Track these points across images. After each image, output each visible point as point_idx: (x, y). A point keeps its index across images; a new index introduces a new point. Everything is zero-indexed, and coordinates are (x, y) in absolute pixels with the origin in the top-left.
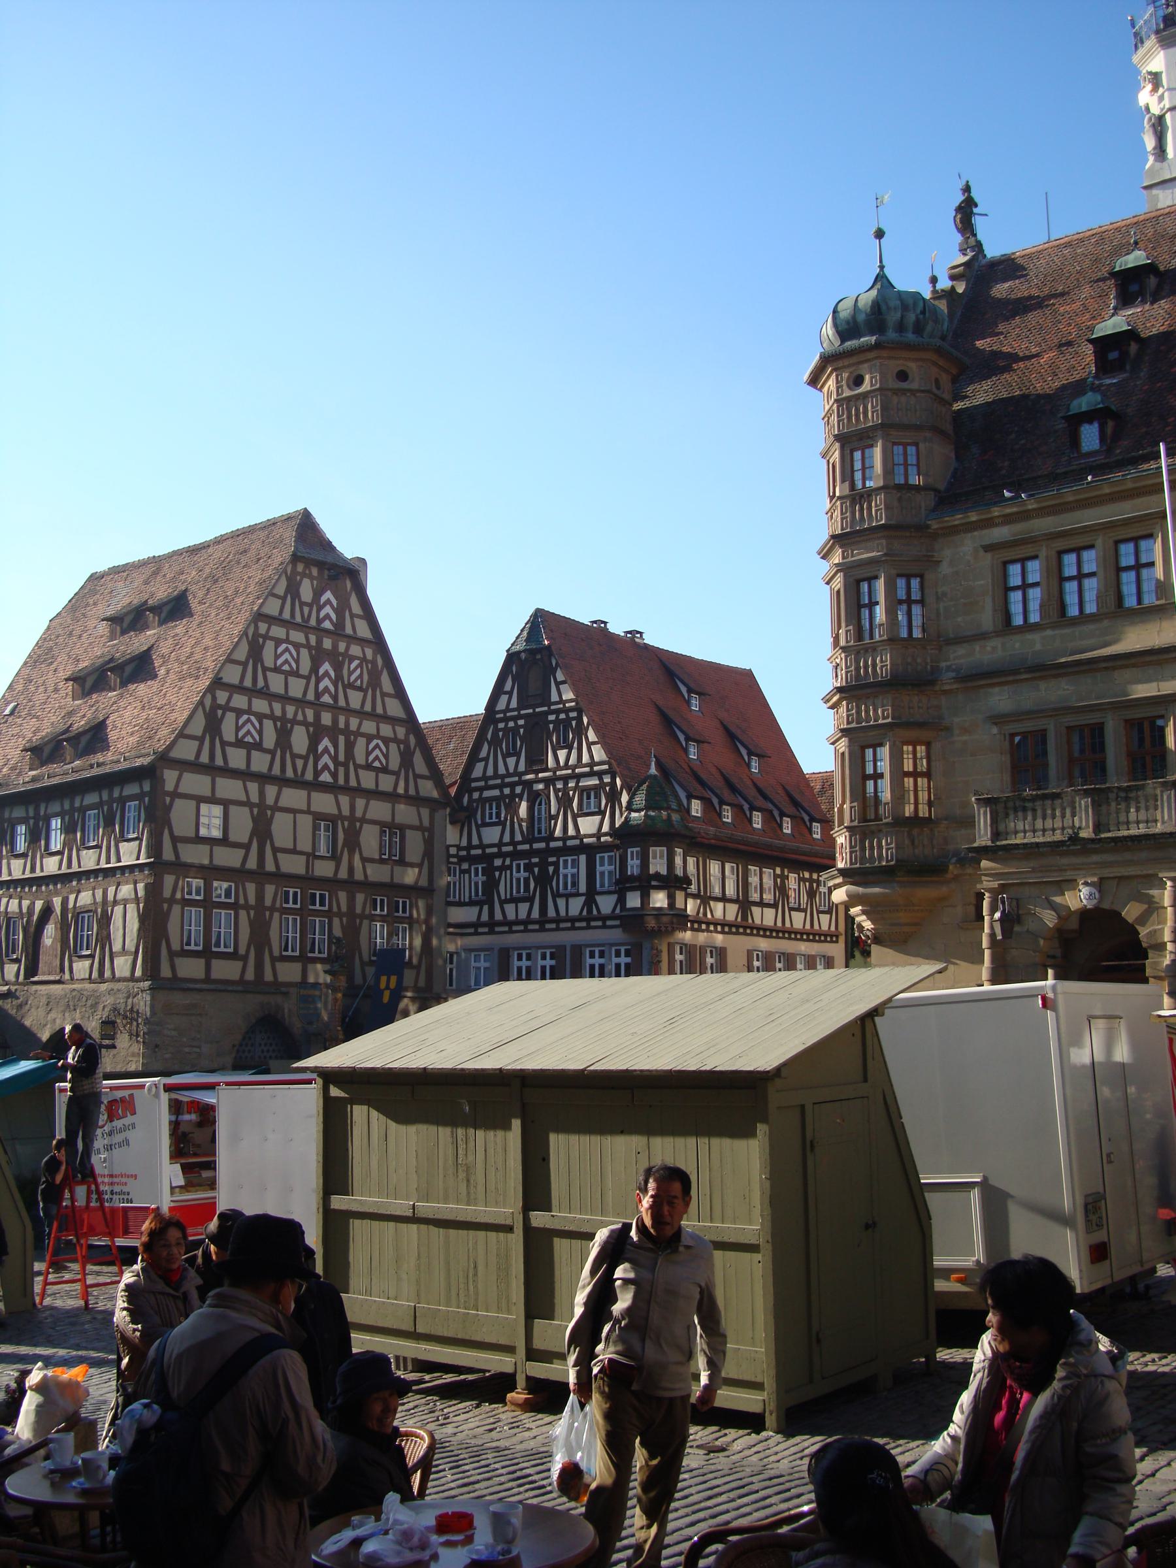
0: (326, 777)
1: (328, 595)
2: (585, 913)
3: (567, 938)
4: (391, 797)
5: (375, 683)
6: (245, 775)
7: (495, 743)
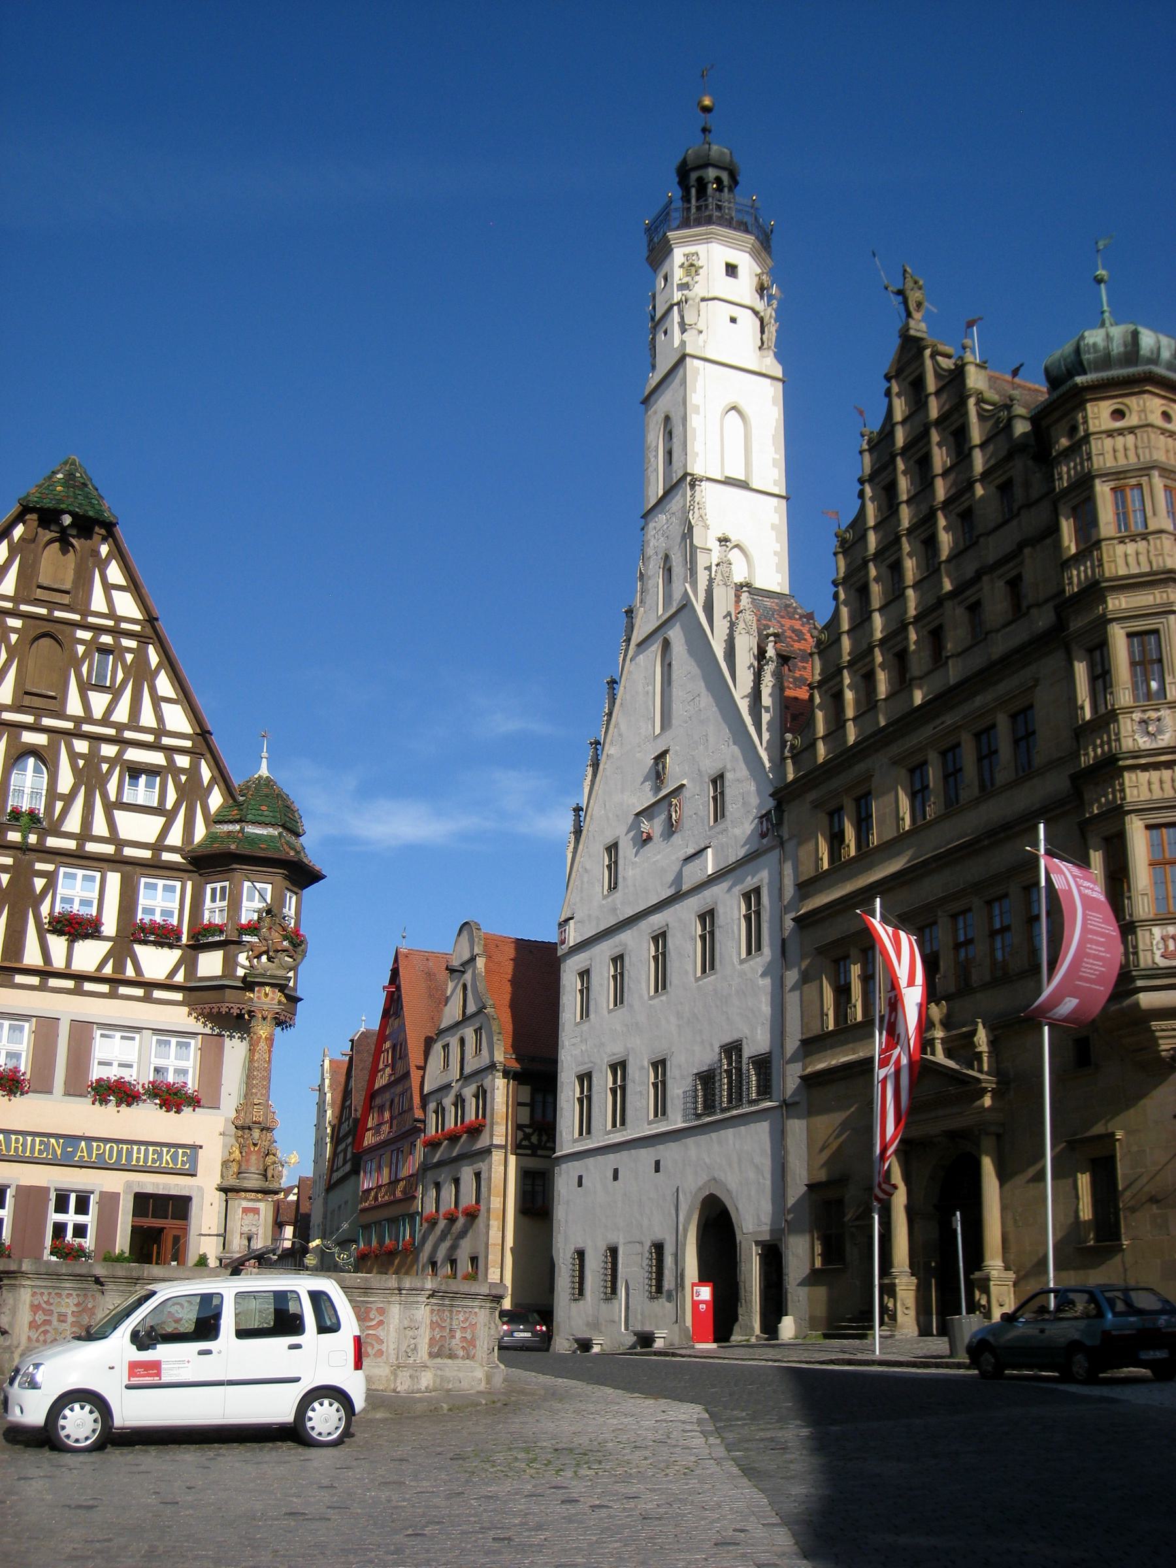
2: (108, 970)
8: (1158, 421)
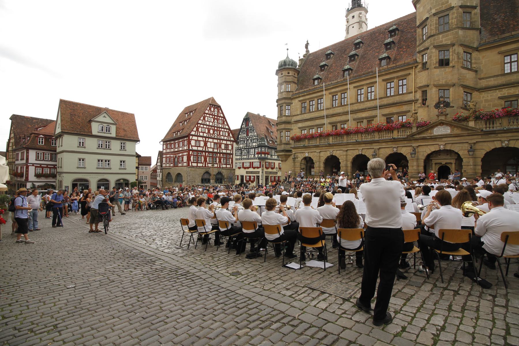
0: (216, 137)
1: (216, 110)
3: (251, 161)
4: (226, 140)
5: (224, 123)
6: (203, 137)
7: (242, 132)
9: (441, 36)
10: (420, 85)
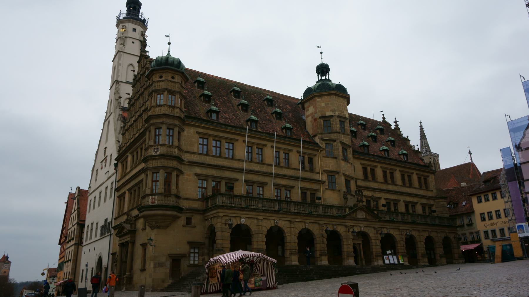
8: (170, 79)
9: (343, 136)
10: (326, 169)
